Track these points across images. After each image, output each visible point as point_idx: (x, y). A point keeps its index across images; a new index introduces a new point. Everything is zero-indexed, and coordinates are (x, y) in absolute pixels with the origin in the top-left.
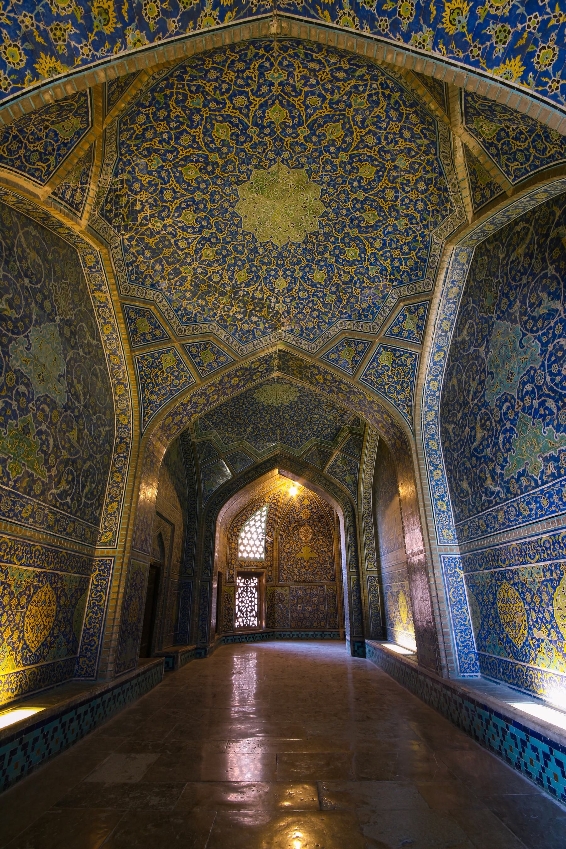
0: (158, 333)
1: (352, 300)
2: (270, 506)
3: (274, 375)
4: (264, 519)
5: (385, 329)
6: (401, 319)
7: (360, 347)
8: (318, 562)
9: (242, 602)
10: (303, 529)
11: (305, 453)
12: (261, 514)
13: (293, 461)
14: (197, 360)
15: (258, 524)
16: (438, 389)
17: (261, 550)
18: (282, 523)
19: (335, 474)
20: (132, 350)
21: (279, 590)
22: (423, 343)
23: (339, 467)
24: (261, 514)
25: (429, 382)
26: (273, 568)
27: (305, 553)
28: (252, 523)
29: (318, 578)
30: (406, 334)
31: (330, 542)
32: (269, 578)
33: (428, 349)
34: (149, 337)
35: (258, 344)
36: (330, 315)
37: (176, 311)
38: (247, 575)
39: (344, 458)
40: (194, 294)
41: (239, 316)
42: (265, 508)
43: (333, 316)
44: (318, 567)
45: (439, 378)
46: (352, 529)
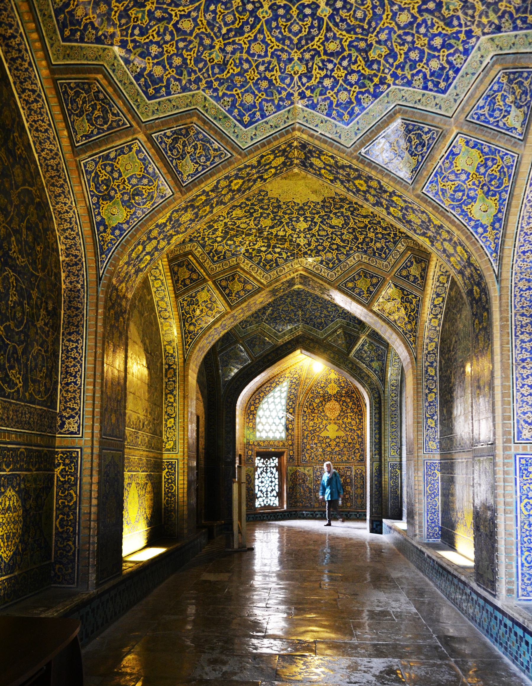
0: (194, 276)
1: (367, 240)
2: (291, 382)
3: (296, 287)
4: (284, 395)
5: (395, 270)
6: (409, 264)
7: (375, 281)
8: (346, 441)
9: (262, 482)
10: (328, 405)
11: (329, 335)
12: (280, 391)
13: (317, 342)
14: (227, 291)
15: (277, 400)
16: (439, 325)
17: (282, 428)
18: (305, 402)
19: (361, 359)
20: (176, 297)
21: (301, 469)
22: (424, 290)
23: (366, 352)
24: (280, 391)
25: (431, 320)
26: (295, 447)
27: (331, 431)
28: (270, 400)
29: (345, 458)
30: (412, 278)
31: (360, 420)
32: (291, 458)
33: (428, 296)
34: (188, 282)
35: (281, 271)
36: (347, 248)
37: (209, 254)
38: (266, 455)
39: (371, 344)
40: (224, 238)
41: (263, 249)
42: (285, 384)
43: (351, 249)
44: (345, 447)
45: (439, 316)
46: (377, 416)
